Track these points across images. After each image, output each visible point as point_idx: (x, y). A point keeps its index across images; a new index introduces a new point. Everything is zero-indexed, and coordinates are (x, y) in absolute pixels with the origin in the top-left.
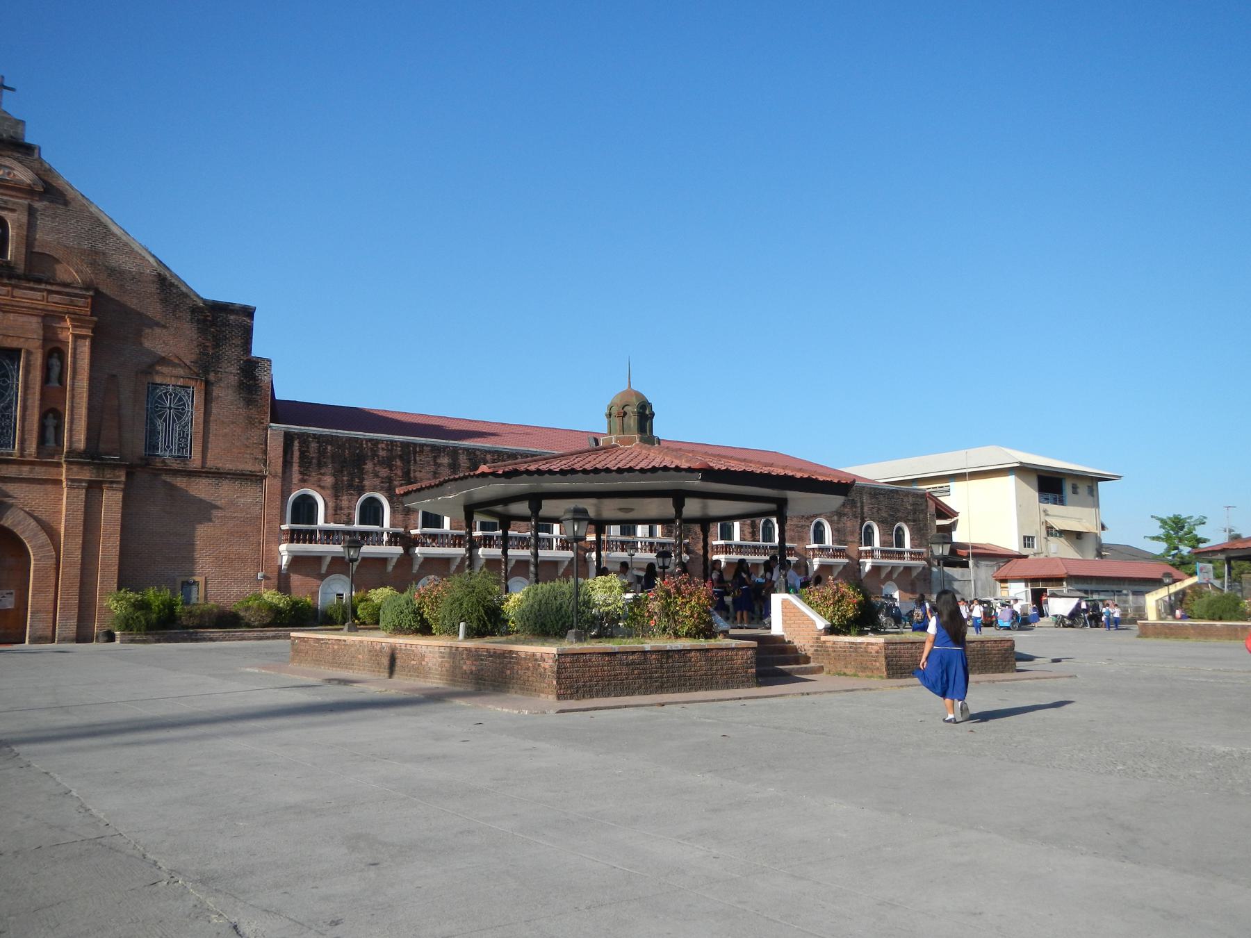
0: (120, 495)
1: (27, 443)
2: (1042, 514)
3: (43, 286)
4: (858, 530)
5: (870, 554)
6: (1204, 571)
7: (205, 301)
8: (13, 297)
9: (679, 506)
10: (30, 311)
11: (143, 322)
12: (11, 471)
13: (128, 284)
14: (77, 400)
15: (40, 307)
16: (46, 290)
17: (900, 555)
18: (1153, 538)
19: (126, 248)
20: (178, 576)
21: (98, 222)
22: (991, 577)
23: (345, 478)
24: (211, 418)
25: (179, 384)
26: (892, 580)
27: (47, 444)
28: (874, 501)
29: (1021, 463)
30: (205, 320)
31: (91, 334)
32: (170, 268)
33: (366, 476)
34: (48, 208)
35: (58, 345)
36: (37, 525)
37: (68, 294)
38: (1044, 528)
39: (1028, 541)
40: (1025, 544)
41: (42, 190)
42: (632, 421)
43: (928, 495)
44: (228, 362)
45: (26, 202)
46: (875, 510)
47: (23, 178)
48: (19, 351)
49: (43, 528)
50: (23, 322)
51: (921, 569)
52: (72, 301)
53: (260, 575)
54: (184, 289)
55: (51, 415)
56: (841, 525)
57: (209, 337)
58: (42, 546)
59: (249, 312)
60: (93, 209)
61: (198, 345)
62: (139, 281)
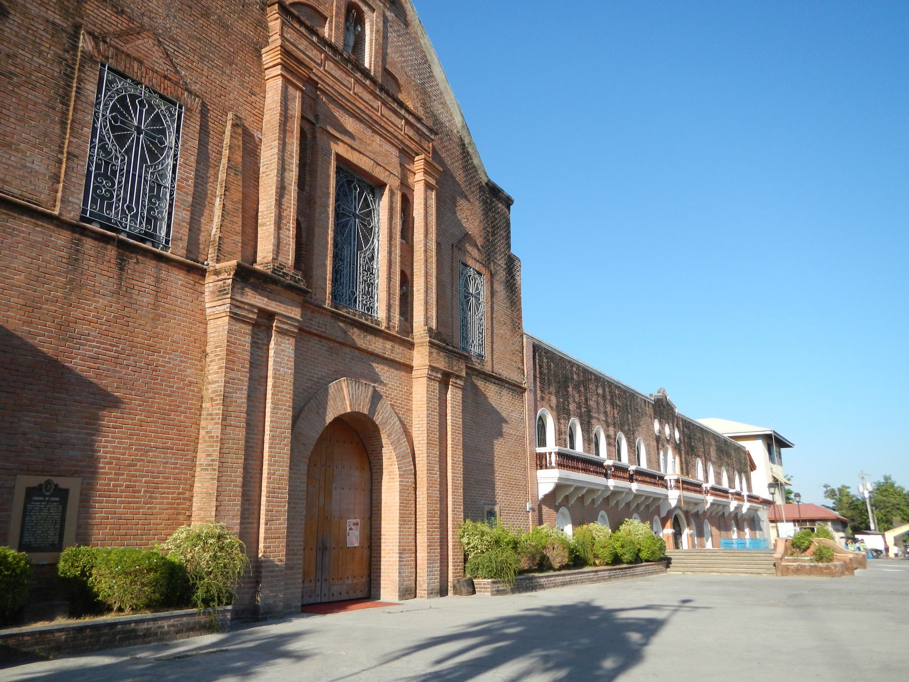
0: (460, 393)
3: (403, 112)
8: (382, 115)
10: (389, 137)
12: (376, 345)
15: (400, 137)
20: (485, 504)
23: (561, 400)
25: (476, 268)
30: (487, 202)
33: (570, 400)
34: (395, 22)
35: (406, 192)
37: (417, 130)
48: (385, 185)
50: (387, 151)
53: (528, 506)
54: (476, 162)
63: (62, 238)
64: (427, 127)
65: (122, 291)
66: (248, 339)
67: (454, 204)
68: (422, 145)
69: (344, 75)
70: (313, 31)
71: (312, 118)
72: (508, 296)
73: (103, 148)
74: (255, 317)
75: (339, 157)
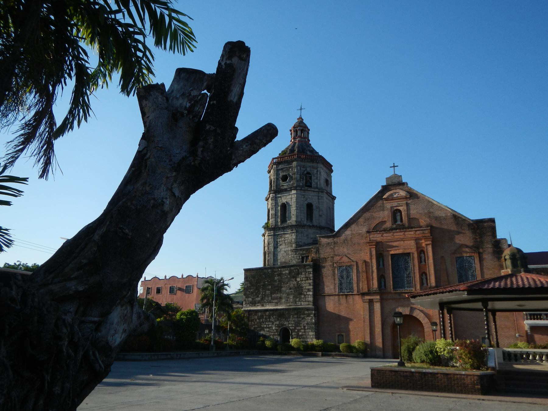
1: (417, 285)
3: (413, 229)
7: (472, 220)
8: (405, 235)
9: (485, 306)
11: (450, 235)
13: (442, 221)
14: (430, 268)
15: (414, 237)
16: (415, 230)
19: (440, 208)
21: (429, 202)
24: (484, 267)
25: (468, 255)
27: (424, 285)
30: (474, 228)
31: (431, 243)
32: (457, 211)
35: (422, 249)
36: (424, 315)
37: (422, 230)
41: (409, 196)
42: (509, 263)
44: (488, 243)
45: (405, 202)
47: (403, 194)
49: (426, 316)
52: (423, 232)
53: (517, 335)
54: (464, 218)
55: (423, 274)
57: (477, 235)
58: (427, 323)
59: (492, 221)
60: (426, 198)
61: (473, 239)
62: (446, 219)
63: (337, 297)
64: (426, 227)
65: (347, 302)
66: (368, 305)
67: (452, 239)
68: (425, 233)
69: (389, 234)
70: (377, 231)
71: (383, 250)
72: (495, 257)
73: (340, 280)
74: (368, 301)
75: (392, 255)
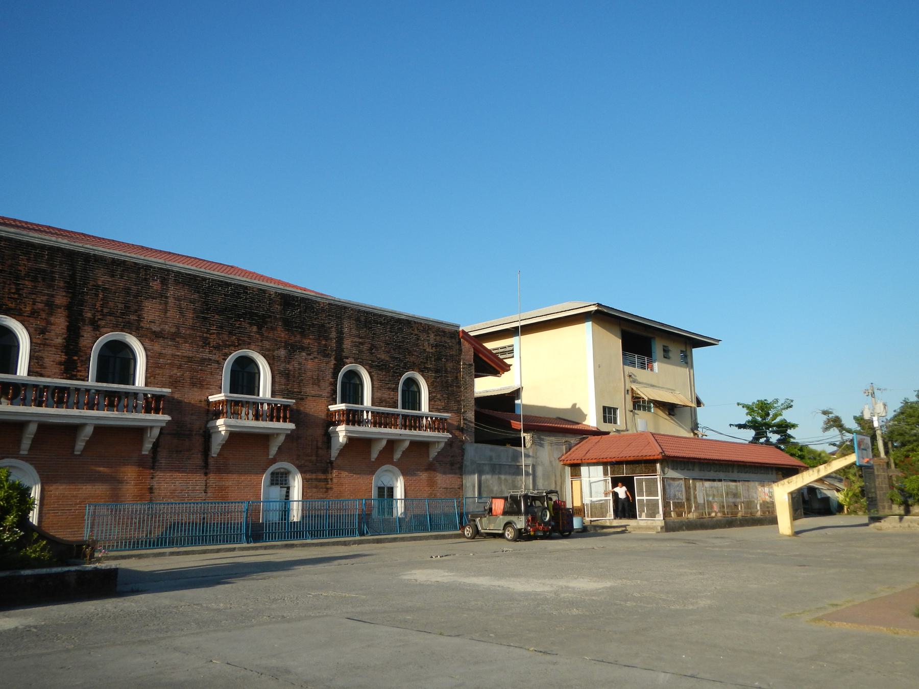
2: (627, 378)
4: (329, 377)
5: (353, 418)
6: (862, 447)
17: (413, 422)
18: (740, 426)
22: (557, 461)
26: (392, 463)
28: (363, 332)
29: (599, 305)
38: (629, 397)
39: (608, 414)
40: (605, 417)
43: (461, 334)
46: (365, 347)
51: (442, 445)
56: (293, 366)
